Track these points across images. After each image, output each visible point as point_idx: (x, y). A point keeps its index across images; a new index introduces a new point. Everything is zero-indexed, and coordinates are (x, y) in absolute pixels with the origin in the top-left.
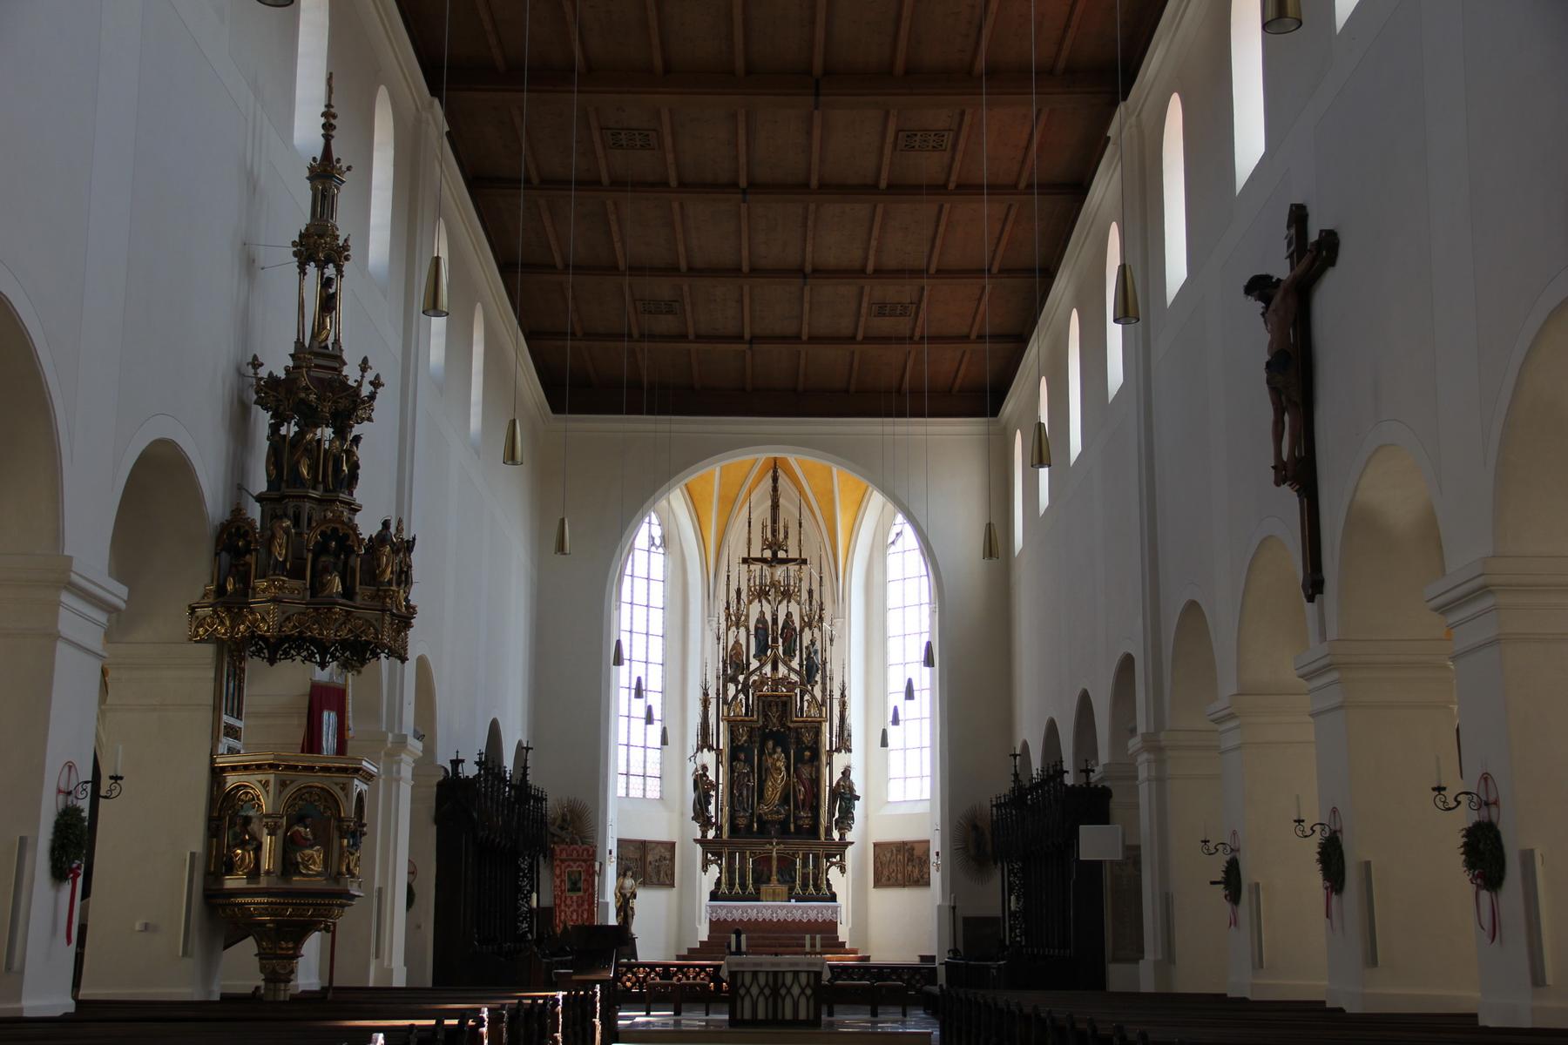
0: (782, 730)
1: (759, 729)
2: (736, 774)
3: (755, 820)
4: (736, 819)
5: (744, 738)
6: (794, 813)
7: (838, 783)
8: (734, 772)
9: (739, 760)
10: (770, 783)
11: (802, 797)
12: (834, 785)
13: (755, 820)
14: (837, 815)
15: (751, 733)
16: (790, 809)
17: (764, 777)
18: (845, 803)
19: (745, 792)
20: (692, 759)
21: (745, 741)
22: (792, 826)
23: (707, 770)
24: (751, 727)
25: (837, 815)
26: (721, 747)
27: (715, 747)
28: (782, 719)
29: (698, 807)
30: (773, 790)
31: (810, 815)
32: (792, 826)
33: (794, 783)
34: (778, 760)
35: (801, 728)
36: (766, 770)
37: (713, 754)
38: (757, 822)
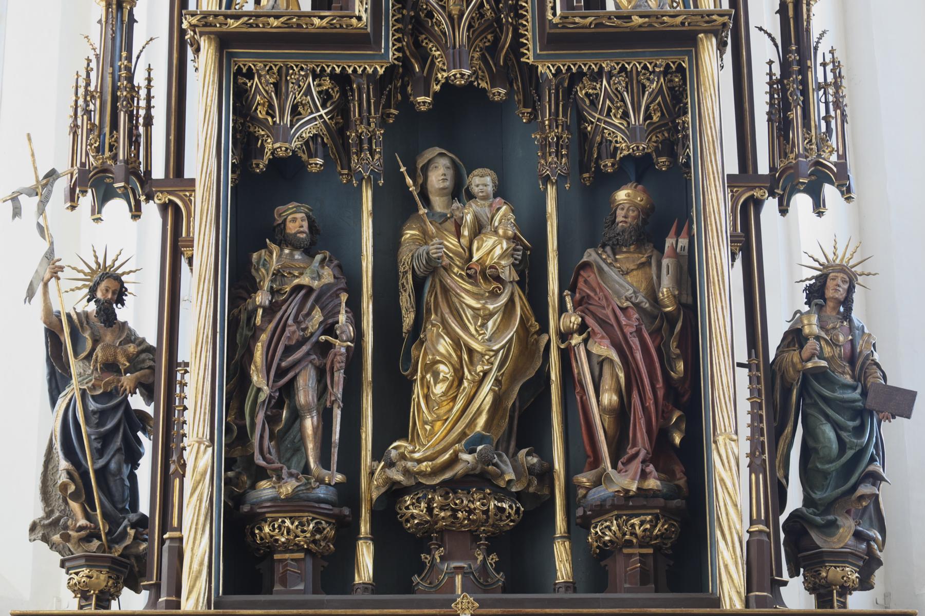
0: (499, 92)
1: (381, 83)
2: (262, 298)
3: (365, 528)
4: (256, 518)
5: (307, 132)
6: (570, 489)
7: (795, 337)
8: (255, 288)
9: (284, 240)
10: (444, 346)
11: (609, 398)
12: (775, 340)
13: (365, 528)
14: (795, 499)
15: (342, 110)
16: (545, 475)
17: (408, 319)
18: (837, 427)
19: (306, 392)
20: (29, 204)
21: (312, 144)
22: (561, 554)
23: (120, 295)
24: (342, 80)
25: (795, 499)
26: (189, 172)
27: (158, 172)
28: (493, 49)
29: (64, 464)
30: (459, 378)
31: (653, 483)
32: (561, 554)
33: (564, 336)
34: (479, 229)
35: (597, 76)
36: (419, 285)
37: (151, 210)
38: (376, 537)
